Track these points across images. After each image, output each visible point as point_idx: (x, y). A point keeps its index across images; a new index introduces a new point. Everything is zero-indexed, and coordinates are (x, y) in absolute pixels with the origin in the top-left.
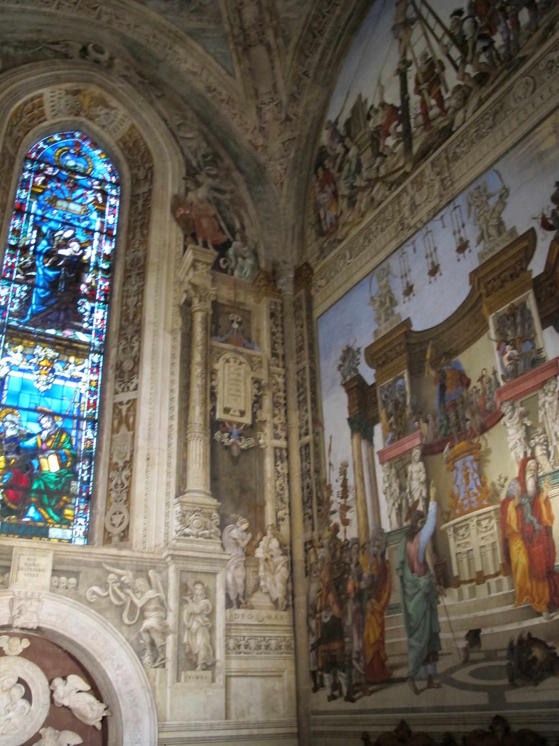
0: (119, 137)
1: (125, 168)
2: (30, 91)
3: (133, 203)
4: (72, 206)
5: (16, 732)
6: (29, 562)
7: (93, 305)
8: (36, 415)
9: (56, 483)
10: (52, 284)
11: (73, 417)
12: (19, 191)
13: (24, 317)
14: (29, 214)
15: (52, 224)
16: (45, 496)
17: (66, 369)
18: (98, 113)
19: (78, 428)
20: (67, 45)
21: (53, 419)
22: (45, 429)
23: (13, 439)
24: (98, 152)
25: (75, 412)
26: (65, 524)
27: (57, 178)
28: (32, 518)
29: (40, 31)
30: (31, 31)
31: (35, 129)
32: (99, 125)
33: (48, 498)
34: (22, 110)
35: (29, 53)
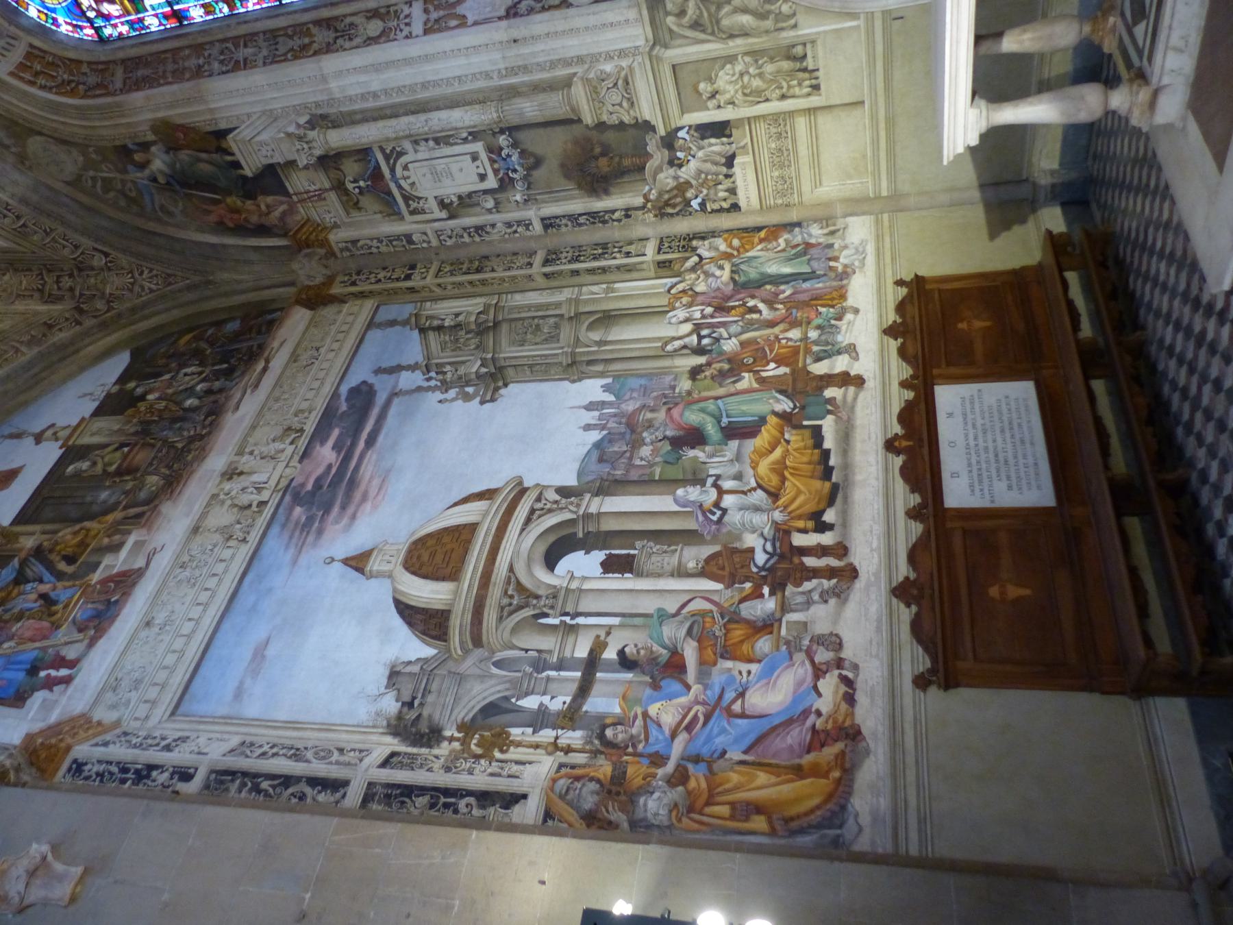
2: (25, 93)
31: (60, 53)
34: (56, 87)
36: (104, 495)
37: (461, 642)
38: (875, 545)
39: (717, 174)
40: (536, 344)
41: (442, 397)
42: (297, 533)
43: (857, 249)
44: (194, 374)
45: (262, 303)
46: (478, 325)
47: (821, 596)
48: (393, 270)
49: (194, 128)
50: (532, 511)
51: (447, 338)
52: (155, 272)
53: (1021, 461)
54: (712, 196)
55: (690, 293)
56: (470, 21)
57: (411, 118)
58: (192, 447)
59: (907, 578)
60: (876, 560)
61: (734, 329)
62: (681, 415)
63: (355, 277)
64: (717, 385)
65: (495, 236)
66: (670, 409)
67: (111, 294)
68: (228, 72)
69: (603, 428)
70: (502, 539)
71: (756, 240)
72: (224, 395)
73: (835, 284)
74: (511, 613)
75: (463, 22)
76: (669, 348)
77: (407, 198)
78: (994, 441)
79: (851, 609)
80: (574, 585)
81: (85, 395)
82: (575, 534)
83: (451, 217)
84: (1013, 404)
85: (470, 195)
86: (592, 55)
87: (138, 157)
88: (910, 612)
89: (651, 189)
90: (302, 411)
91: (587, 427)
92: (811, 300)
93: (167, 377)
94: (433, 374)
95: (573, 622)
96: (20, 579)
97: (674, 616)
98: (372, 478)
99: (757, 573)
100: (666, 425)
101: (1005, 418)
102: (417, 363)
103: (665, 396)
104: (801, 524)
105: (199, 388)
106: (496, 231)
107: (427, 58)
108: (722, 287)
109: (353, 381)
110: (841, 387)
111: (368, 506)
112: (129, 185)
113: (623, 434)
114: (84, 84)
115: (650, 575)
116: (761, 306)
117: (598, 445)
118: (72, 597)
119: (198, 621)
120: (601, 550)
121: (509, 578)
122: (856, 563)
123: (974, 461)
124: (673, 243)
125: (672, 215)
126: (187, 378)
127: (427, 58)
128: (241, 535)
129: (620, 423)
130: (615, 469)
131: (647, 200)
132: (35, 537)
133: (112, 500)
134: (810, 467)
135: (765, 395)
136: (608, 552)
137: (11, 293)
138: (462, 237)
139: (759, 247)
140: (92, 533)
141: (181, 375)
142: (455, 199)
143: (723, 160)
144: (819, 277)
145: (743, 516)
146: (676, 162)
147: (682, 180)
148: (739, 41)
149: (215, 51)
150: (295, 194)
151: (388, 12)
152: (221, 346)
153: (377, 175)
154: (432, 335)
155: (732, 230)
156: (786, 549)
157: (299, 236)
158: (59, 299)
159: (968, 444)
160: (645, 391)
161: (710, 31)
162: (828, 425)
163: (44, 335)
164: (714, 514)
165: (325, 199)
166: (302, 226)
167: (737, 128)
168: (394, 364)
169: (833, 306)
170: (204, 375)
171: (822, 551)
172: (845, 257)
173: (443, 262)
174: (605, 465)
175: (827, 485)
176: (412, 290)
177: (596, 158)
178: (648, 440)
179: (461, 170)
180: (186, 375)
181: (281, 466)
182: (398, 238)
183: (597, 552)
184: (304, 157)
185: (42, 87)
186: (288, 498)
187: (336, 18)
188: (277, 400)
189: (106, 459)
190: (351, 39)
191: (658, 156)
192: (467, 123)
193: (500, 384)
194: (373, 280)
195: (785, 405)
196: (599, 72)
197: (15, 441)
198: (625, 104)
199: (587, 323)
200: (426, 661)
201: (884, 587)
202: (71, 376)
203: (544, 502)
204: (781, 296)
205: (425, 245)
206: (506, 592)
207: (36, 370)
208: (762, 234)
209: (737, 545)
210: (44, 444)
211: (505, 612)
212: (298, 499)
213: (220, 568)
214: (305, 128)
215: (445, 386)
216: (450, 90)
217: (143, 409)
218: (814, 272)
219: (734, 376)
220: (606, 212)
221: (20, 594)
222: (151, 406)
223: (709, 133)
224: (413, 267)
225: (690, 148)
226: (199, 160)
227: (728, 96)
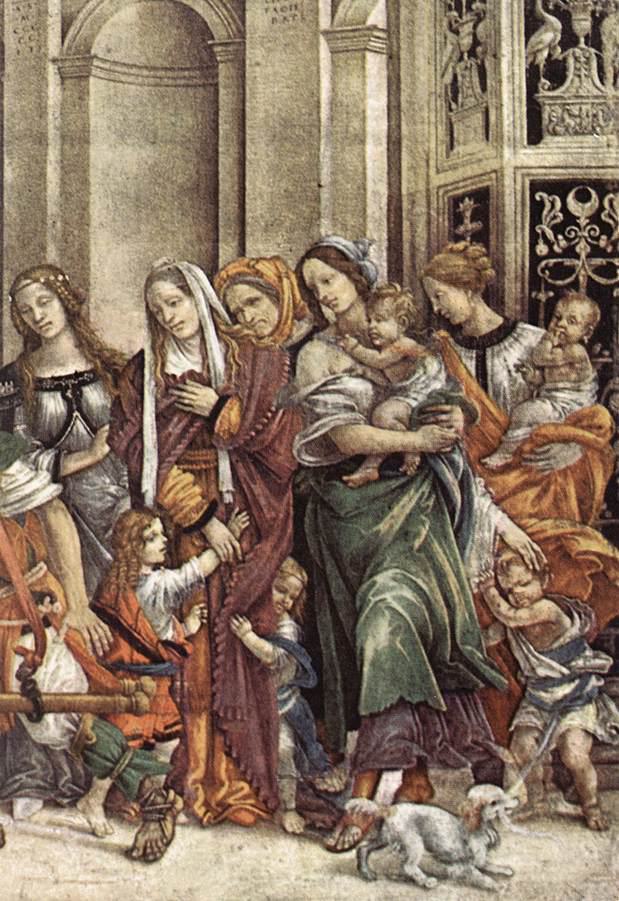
116: (201, 565)
172: (419, 823)
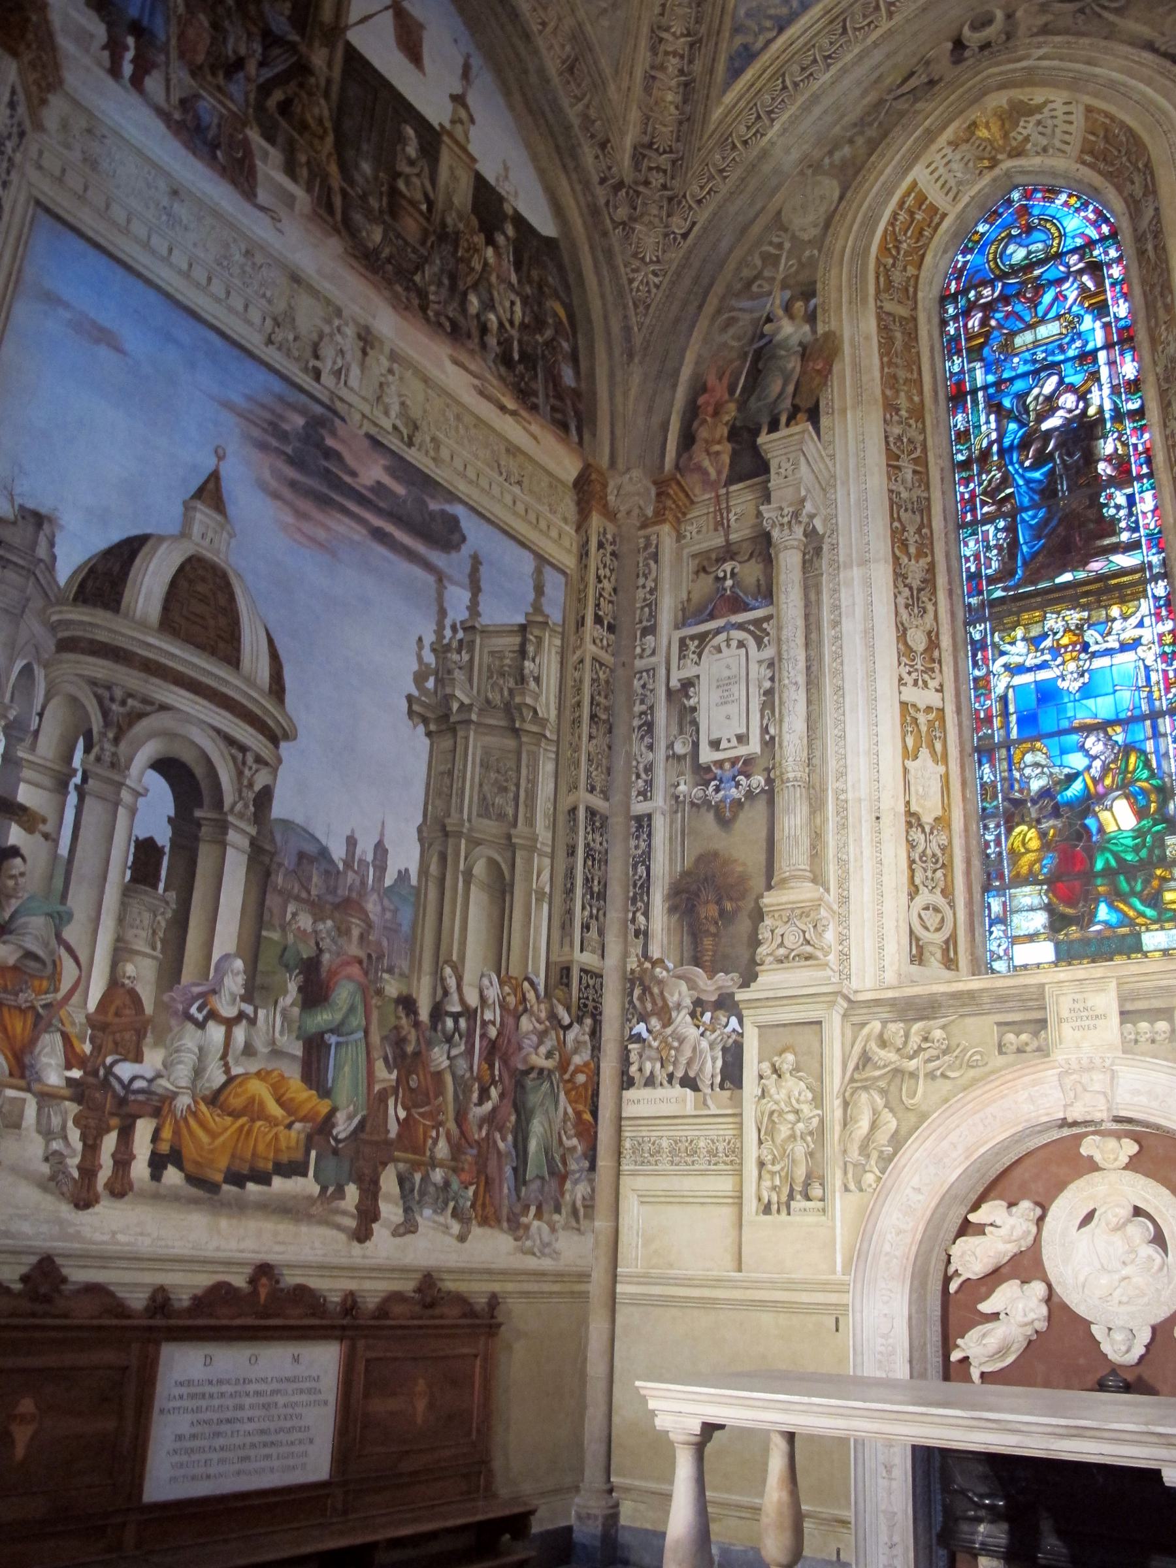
0: (1078, 146)
1: (1111, 194)
2: (890, 194)
3: (1141, 253)
4: (1043, 331)
5: (1146, 1299)
6: (1077, 1006)
7: (1129, 491)
8: (1074, 738)
9: (1136, 849)
10: (1047, 492)
11: (1142, 718)
12: (948, 364)
13: (1012, 573)
14: (974, 392)
15: (1019, 385)
16: (1122, 878)
17: (1109, 634)
18: (1025, 133)
19: (1156, 734)
20: (928, 63)
21: (1106, 733)
22: (1095, 758)
23: (1045, 793)
24: (1063, 197)
25: (1145, 708)
26: (1168, 921)
27: (1005, 299)
28: (1106, 923)
29: (879, 79)
30: (865, 93)
32: (1038, 153)
33: (1128, 881)
35: (872, 132)
36: (366, 167)
37: (68, 623)
38: (121, 1238)
39: (675, 1064)
40: (481, 785)
41: (427, 643)
42: (268, 416)
43: (548, 1245)
44: (512, 312)
45: (593, 422)
46: (519, 707)
47: (55, 1152)
48: (610, 602)
49: (825, 384)
50: (243, 749)
51: (507, 661)
52: (654, 290)
53: (215, 1456)
54: (647, 1052)
55: (521, 1008)
56: (909, 763)
57: (802, 664)
58: (413, 295)
59: (64, 1280)
60: (98, 1237)
61: (462, 1064)
62: (349, 978)
63: (609, 548)
64: (385, 1033)
65: (637, 747)
66: (360, 962)
67: (633, 230)
68: (887, 443)
69: (348, 864)
70: (210, 701)
71: (580, 1107)
72: (477, 348)
73: (505, 1211)
74: (100, 700)
75: (909, 754)
76: (448, 971)
77: (703, 638)
78: (250, 1419)
79: (29, 1194)
80: (125, 795)
81: (506, 169)
82: (200, 805)
83: (669, 692)
84: (296, 1449)
85: (695, 723)
86: (847, 917)
87: (799, 305)
88: (12, 1281)
89: (668, 970)
90: (437, 448)
91: (351, 842)
92: (487, 1178)
93: (514, 278)
94: (460, 634)
95: (71, 787)
96: (270, 39)
97: (58, 936)
98: (328, 529)
99: (104, 1063)
100: (338, 955)
101: (281, 1437)
102: (479, 614)
103: (380, 957)
104: (167, 1134)
105: (492, 317)
106: (644, 749)
107: (872, 702)
108: (524, 1052)
109: (468, 524)
110: (357, 1208)
111: (290, 519)
112: (766, 288)
113: (333, 891)
114: (894, 265)
115: (124, 905)
116: (488, 1106)
117: (324, 853)
118: (232, 100)
119: (166, 260)
120: (171, 840)
121: (151, 703)
122: (98, 1208)
123: (225, 1388)
124: (591, 991)
125: (631, 994)
126: (508, 304)
127: (872, 702)
128: (279, 336)
129: (351, 889)
130: (285, 875)
131: (654, 964)
132: (325, 69)
133: (358, 178)
134: (249, 1155)
135: (362, 1099)
136: (167, 850)
137: (652, 110)
138: (642, 702)
139: (570, 1110)
140: (316, 142)
141: (513, 297)
142: (692, 702)
143: (692, 1074)
144: (517, 1190)
145: (190, 1051)
146: (699, 1010)
147: (674, 1014)
148: (839, 1114)
149: (913, 433)
150: (728, 493)
151: (933, 661)
152: (544, 356)
153: (737, 605)
154: (517, 640)
155: (598, 1074)
156: (131, 1109)
157: (675, 487)
158: (637, 167)
159: (250, 1381)
160: (391, 930)
161: (856, 1076)
162: (307, 1185)
163: (592, 136)
164: (200, 1009)
165: (716, 530)
166: (687, 495)
167: (731, 1099)
168: (483, 585)
169: (473, 1206)
170: (507, 325)
171: (123, 1161)
172: (539, 1229)
173: (612, 671)
174: (294, 859)
175: (219, 1177)
176: (581, 622)
177: (719, 902)
178: (321, 926)
179: (728, 717)
180: (513, 303)
181: (366, 409)
182: (653, 616)
183: (169, 833)
184: (773, 515)
185: (895, 216)
186: (318, 410)
187: (934, 592)
188: (458, 417)
189: (415, 180)
190: (907, 606)
191: (710, 986)
192: (786, 737)
193: (432, 727)
194: (601, 572)
195: (343, 1127)
196: (825, 922)
197: (460, 71)
198: (782, 951)
199: (499, 858)
200: (51, 567)
201: (59, 1245)
202: (535, 158)
203: (254, 767)
204: (498, 1136)
205: (638, 650)
206: (130, 695)
207: (550, 116)
208: (587, 1116)
209: (149, 1039)
210: (449, 106)
211: (102, 691)
212: (316, 424)
213: (237, 303)
214: (808, 524)
215: (441, 649)
216: (830, 722)
217: (476, 239)
218: (525, 1183)
219: (395, 1059)
220: (647, 905)
221: (249, 35)
222: (476, 250)
223: (729, 1059)
224: (611, 629)
225: (714, 1031)
226: (785, 385)
227: (773, 1091)
